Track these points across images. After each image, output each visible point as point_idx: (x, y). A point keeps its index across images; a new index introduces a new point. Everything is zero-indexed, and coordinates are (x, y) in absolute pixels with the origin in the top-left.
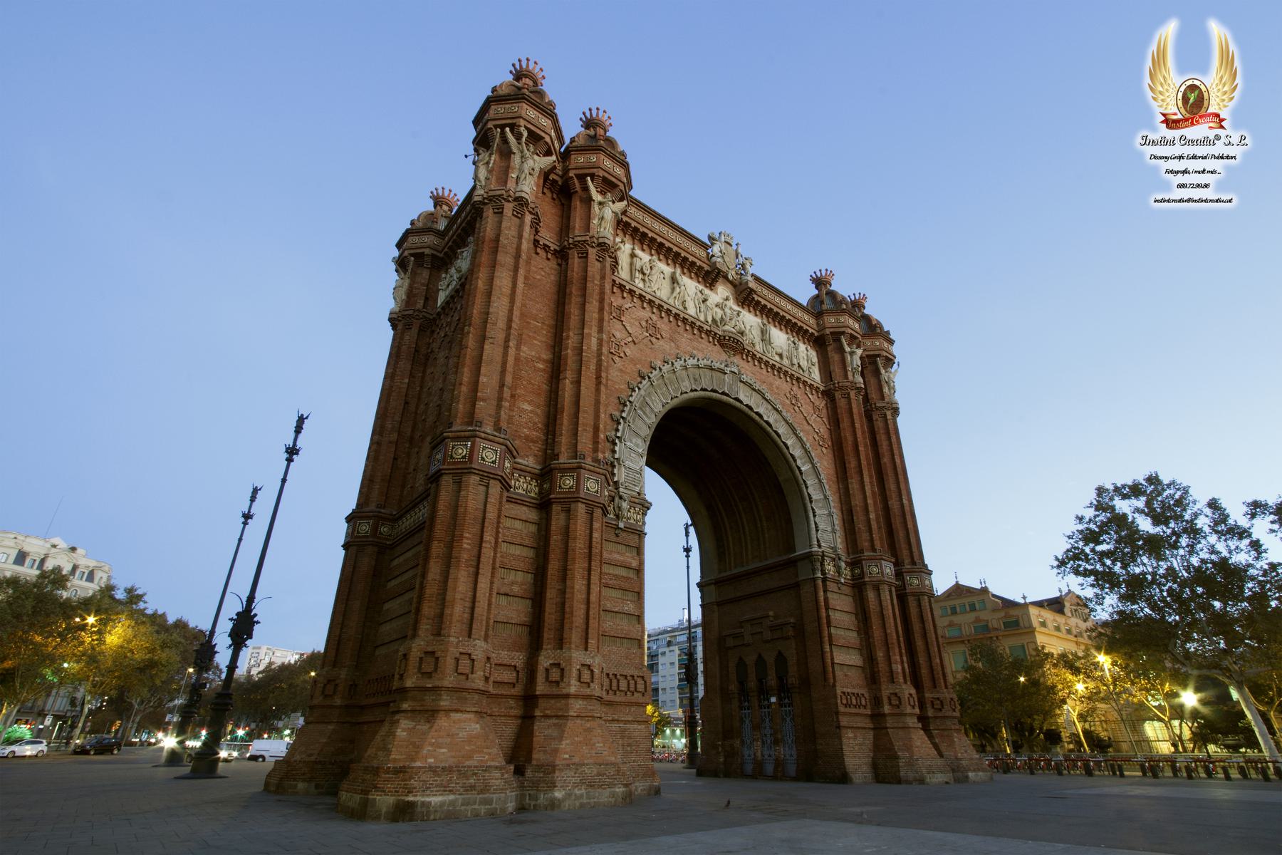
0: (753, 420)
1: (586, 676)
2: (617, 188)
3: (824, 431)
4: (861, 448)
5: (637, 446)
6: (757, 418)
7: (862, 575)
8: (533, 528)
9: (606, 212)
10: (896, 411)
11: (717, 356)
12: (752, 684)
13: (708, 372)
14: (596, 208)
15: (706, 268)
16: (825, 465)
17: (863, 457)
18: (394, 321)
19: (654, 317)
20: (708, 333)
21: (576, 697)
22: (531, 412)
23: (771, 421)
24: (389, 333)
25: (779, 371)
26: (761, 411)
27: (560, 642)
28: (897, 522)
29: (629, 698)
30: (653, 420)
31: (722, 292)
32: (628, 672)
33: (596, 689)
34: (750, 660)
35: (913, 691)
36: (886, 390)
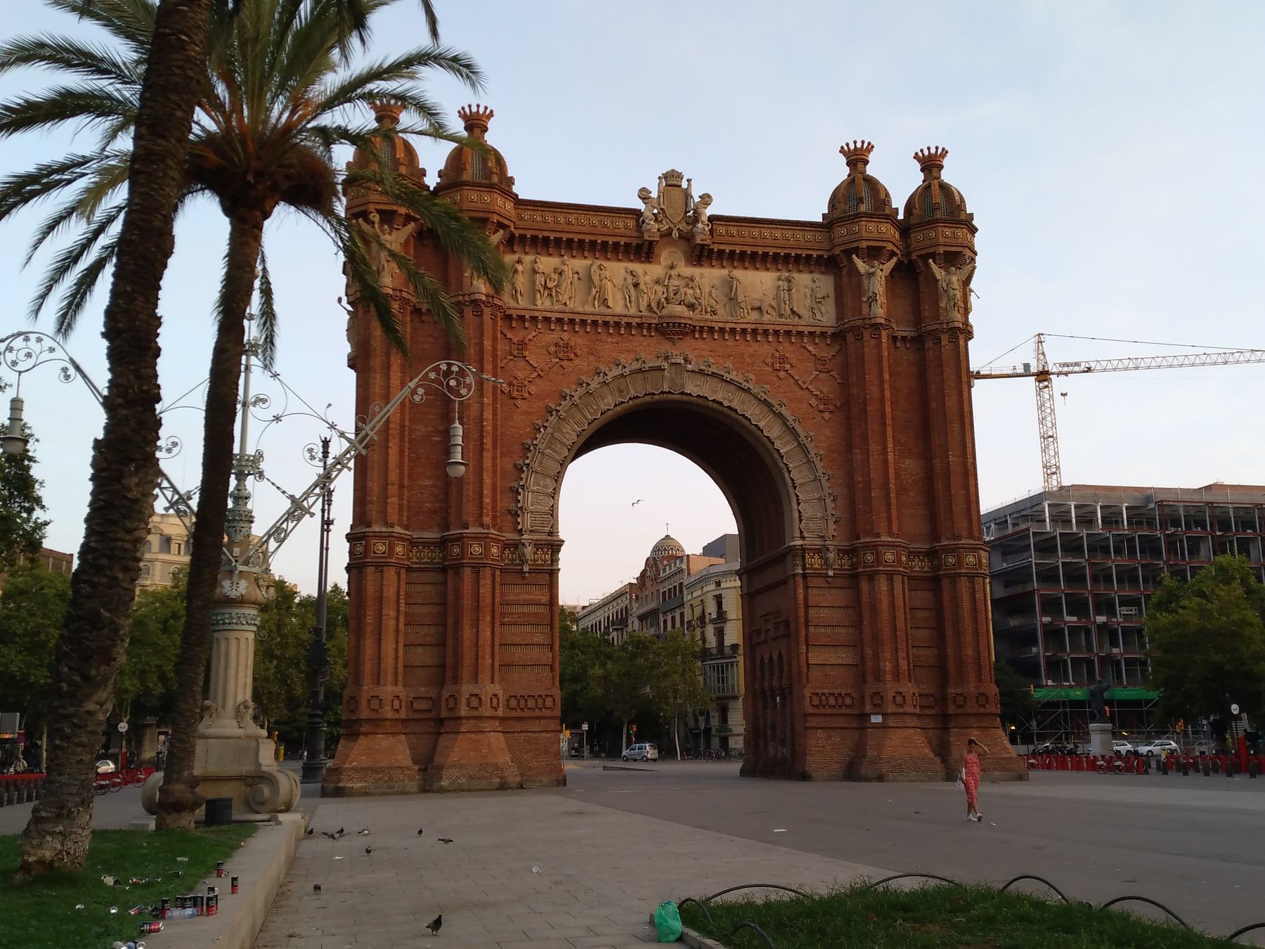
1: (475, 702)
5: (546, 486)
6: (715, 406)
11: (649, 351)
15: (634, 242)
16: (821, 434)
19: (566, 336)
20: (640, 326)
21: (468, 718)
22: (432, 486)
23: (735, 405)
26: (719, 397)
27: (456, 679)
29: (537, 713)
31: (667, 255)
32: (536, 693)
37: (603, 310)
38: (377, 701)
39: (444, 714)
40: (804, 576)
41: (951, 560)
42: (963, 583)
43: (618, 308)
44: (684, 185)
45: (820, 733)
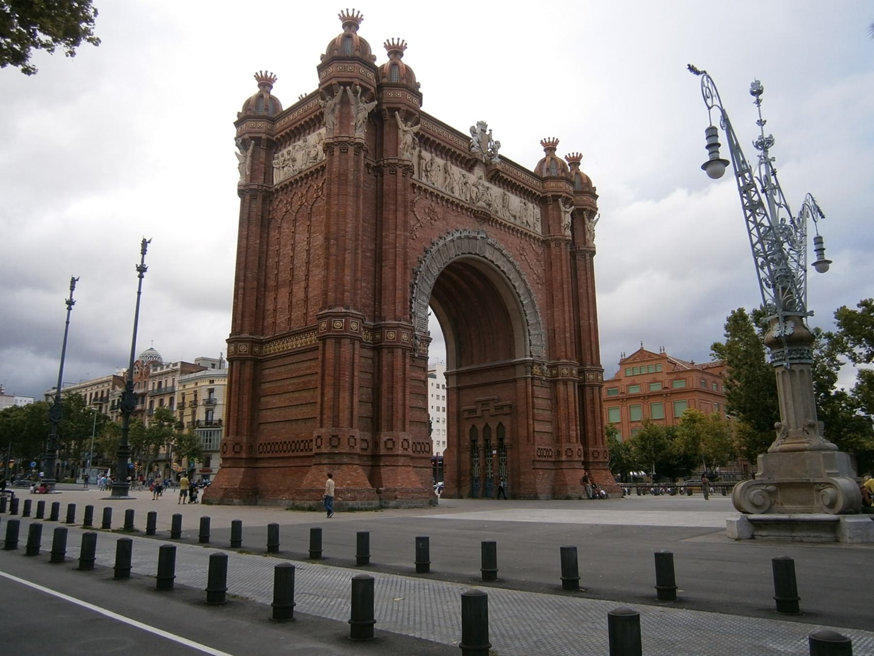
0: (493, 269)
2: (415, 115)
3: (539, 270)
4: (565, 286)
6: (496, 268)
7: (557, 375)
8: (370, 361)
9: (407, 134)
10: (594, 253)
12: (480, 442)
13: (467, 240)
14: (401, 133)
15: (468, 157)
16: (539, 298)
17: (565, 292)
18: (241, 193)
20: (467, 209)
21: (401, 456)
23: (505, 270)
24: (238, 200)
25: (513, 230)
26: (499, 263)
27: (391, 428)
28: (584, 335)
29: (422, 455)
30: (432, 282)
31: (479, 171)
32: (421, 441)
33: (410, 452)
34: (480, 427)
35: (581, 447)
36: (588, 236)
37: (449, 193)
38: (336, 439)
39: (383, 451)
40: (532, 379)
41: (591, 377)
42: (596, 390)
43: (457, 195)
44: (488, 133)
45: (541, 472)
